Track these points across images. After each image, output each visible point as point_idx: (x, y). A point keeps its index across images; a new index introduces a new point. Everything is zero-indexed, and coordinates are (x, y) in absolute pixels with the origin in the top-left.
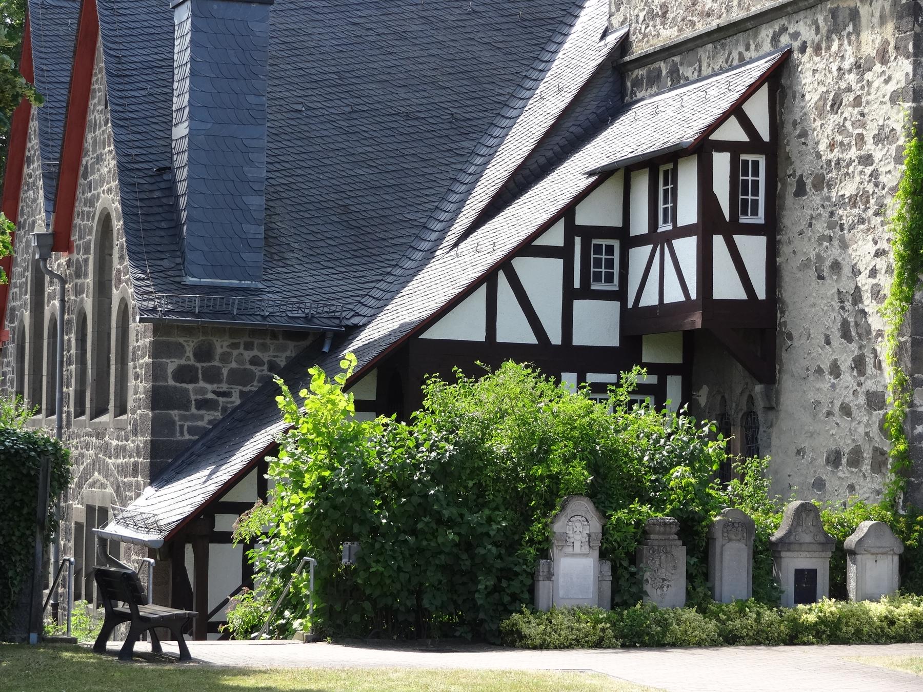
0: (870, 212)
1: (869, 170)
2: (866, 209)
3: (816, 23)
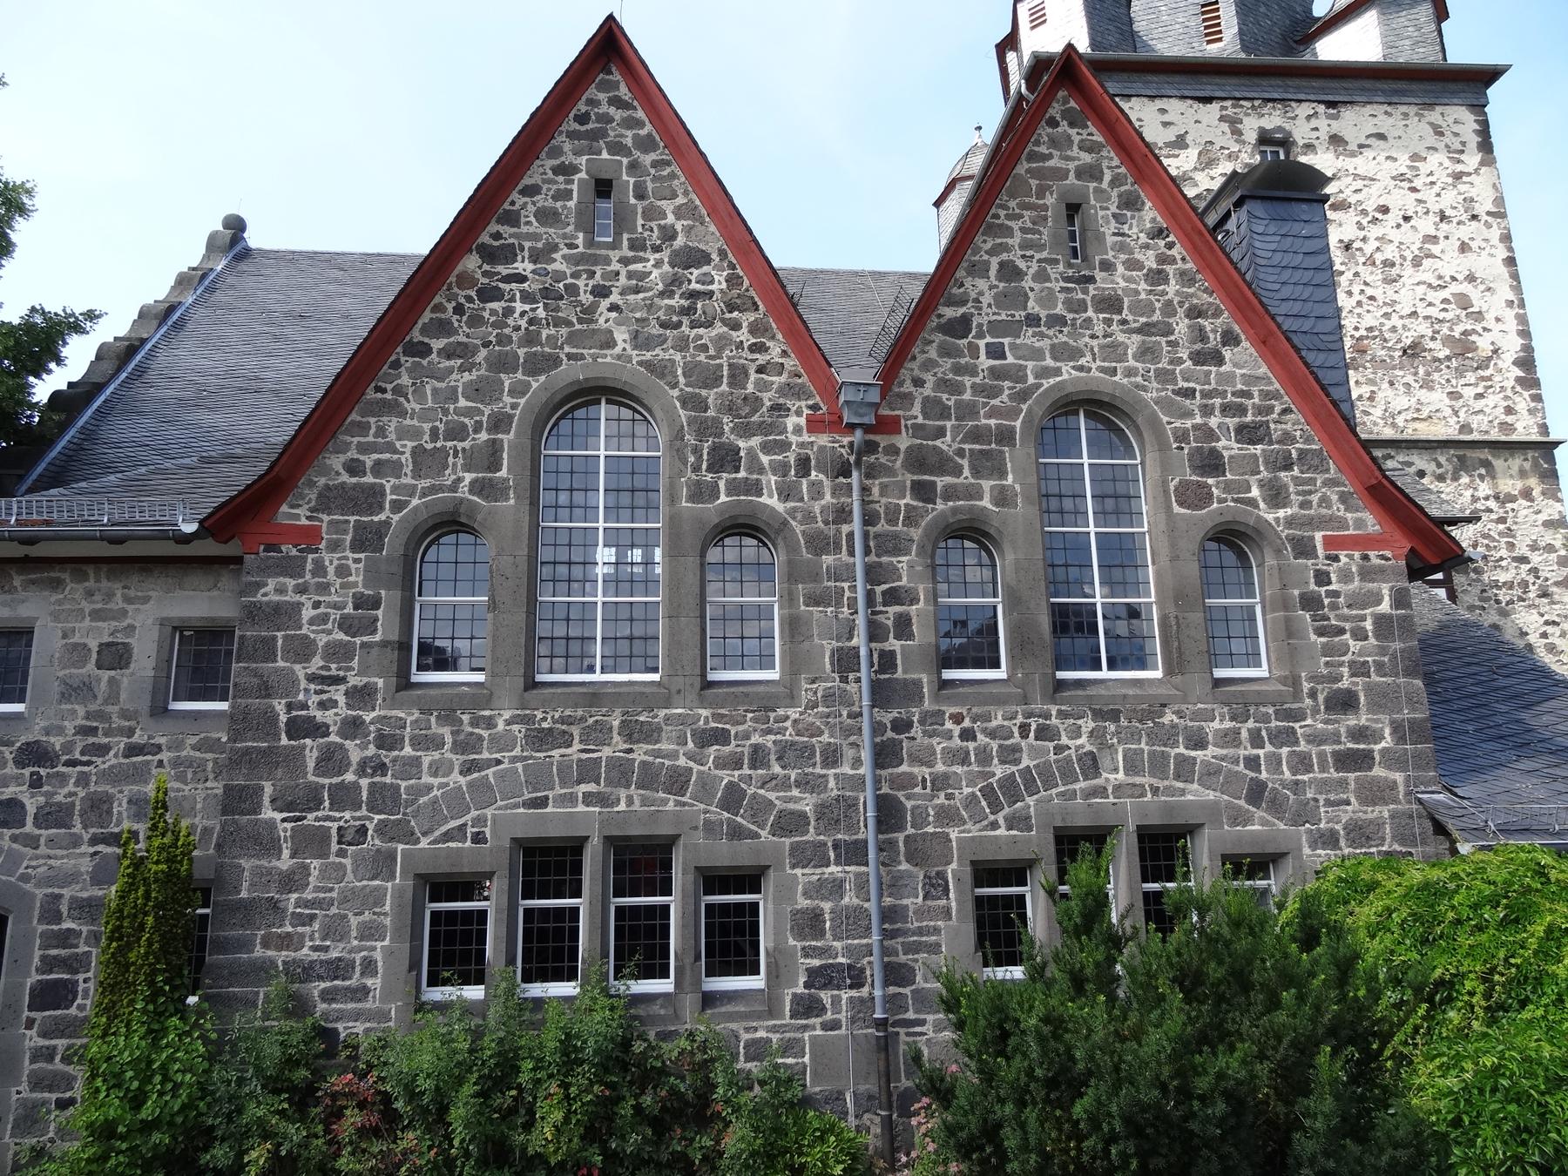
2: (1525, 592)
3: (1435, 460)
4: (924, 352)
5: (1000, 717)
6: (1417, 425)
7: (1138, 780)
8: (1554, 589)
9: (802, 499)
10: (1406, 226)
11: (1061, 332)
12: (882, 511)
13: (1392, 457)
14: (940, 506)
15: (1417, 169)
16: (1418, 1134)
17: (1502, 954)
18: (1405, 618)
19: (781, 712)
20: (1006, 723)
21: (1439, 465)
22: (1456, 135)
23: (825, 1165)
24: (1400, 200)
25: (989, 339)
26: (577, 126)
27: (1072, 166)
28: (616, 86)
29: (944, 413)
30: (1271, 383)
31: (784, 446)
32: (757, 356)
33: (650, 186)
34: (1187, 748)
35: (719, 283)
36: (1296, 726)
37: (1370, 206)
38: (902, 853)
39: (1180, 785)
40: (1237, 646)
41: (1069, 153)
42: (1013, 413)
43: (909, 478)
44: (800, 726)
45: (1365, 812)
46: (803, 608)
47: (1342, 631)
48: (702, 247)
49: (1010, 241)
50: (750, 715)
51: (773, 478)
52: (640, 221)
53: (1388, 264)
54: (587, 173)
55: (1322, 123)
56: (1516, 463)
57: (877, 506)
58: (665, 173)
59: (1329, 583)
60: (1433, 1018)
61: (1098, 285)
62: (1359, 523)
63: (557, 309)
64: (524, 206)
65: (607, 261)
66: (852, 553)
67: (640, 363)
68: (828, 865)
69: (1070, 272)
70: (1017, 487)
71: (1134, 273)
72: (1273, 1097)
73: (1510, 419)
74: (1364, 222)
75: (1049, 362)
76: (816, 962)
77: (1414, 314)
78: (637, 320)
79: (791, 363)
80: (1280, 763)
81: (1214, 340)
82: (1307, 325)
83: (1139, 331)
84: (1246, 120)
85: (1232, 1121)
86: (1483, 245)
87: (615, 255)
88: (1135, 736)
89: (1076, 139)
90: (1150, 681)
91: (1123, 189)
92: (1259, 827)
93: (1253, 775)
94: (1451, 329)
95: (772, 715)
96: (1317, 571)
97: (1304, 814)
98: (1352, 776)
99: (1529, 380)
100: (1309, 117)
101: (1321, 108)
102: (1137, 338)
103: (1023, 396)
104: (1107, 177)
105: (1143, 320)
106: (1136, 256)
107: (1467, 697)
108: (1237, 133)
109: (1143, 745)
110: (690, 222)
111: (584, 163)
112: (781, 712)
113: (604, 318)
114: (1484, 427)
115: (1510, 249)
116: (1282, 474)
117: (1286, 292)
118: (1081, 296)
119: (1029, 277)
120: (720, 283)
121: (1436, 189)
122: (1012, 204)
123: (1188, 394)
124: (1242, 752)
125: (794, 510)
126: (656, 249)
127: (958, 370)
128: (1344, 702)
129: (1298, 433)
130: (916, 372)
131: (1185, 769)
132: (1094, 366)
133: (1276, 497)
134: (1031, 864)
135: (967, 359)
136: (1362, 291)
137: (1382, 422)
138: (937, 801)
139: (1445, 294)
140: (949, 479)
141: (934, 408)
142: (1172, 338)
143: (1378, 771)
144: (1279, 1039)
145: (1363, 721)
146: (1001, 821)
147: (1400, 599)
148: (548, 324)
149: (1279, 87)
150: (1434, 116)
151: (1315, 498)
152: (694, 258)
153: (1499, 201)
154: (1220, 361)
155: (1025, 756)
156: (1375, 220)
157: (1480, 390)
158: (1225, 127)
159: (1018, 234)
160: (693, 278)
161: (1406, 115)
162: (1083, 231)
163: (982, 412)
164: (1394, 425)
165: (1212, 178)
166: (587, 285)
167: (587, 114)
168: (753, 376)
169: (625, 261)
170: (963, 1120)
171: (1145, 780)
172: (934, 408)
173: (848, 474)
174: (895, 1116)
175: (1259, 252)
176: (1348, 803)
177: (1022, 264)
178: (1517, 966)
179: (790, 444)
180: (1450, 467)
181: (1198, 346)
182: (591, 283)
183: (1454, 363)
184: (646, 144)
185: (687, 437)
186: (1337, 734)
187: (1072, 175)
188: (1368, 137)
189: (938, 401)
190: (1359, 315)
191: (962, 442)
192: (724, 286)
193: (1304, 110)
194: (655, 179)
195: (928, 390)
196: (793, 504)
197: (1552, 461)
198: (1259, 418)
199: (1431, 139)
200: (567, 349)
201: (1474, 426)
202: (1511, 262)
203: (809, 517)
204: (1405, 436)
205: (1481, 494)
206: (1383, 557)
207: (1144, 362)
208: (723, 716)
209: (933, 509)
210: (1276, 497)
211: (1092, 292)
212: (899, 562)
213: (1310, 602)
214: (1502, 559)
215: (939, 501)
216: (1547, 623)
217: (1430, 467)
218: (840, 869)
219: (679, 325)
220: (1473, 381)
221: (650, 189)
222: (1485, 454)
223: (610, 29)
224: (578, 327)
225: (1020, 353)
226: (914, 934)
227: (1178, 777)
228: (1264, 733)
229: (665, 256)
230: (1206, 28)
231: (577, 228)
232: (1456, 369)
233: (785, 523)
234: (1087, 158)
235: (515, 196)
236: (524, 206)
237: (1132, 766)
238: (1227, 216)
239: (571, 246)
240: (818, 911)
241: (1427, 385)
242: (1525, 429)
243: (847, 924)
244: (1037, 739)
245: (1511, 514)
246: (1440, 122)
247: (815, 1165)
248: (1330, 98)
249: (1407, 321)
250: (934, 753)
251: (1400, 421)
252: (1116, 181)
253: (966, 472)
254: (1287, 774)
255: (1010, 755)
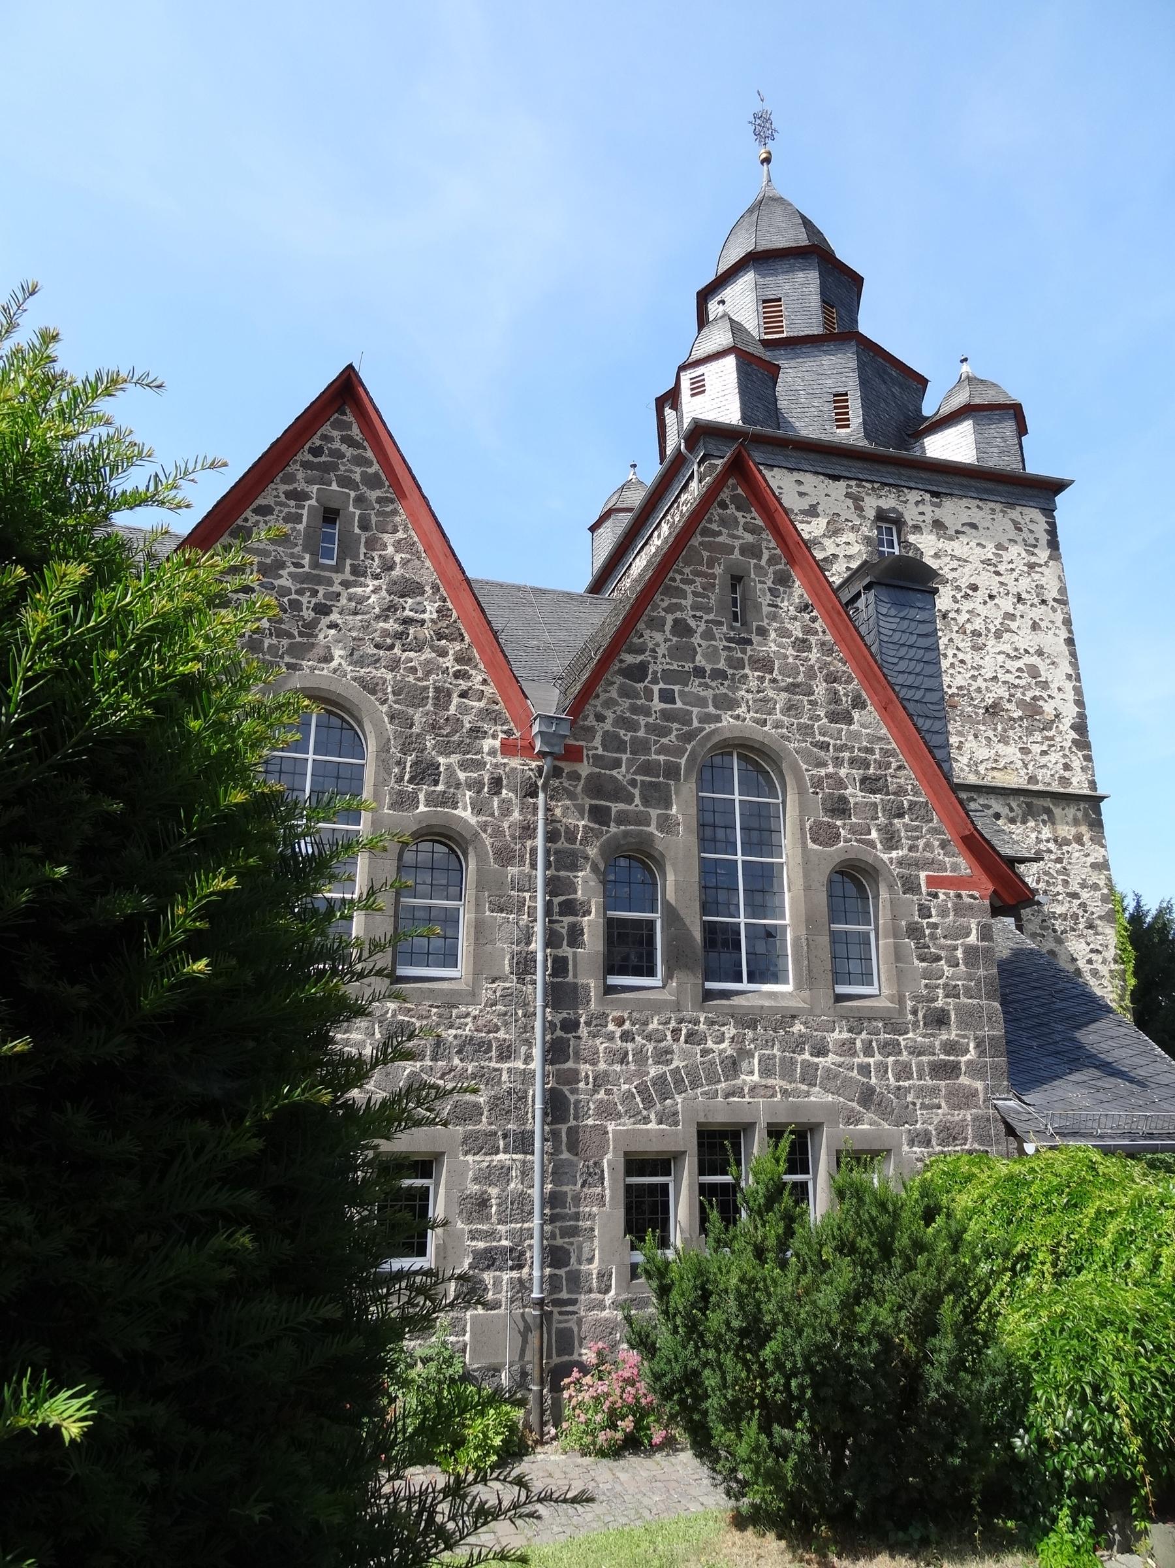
0: (1081, 926)
1: (1076, 902)
2: (1076, 924)
3: (1009, 805)
4: (606, 691)
5: (655, 1021)
6: (995, 774)
7: (770, 1082)
8: (1098, 922)
9: (492, 815)
10: (991, 604)
11: (722, 684)
12: (562, 830)
13: (975, 800)
14: (613, 829)
15: (1001, 556)
16: (1009, 1365)
17: (1065, 1233)
18: (987, 950)
19: (463, 1009)
20: (660, 1027)
21: (1012, 810)
22: (1031, 531)
23: (486, 1436)
24: (986, 581)
25: (662, 685)
26: (311, 458)
27: (737, 543)
28: (349, 426)
29: (621, 747)
30: (889, 743)
31: (480, 765)
32: (461, 682)
33: (374, 519)
34: (812, 1055)
35: (430, 612)
36: (901, 1038)
37: (963, 583)
38: (564, 1144)
39: (805, 1087)
40: (854, 966)
41: (735, 532)
42: (679, 752)
43: (588, 802)
44: (479, 1022)
45: (953, 1115)
46: (488, 913)
47: (938, 958)
48: (416, 578)
49: (683, 602)
50: (434, 1010)
51: (468, 794)
52: (363, 550)
53: (976, 634)
54: (317, 501)
55: (927, 509)
56: (1071, 812)
57: (559, 825)
58: (388, 509)
59: (930, 916)
60: (1014, 1283)
61: (754, 646)
62: (955, 866)
63: (281, 621)
64: (256, 524)
65: (330, 583)
66: (534, 866)
67: (355, 679)
68: (497, 1153)
69: (732, 634)
70: (680, 818)
71: (784, 640)
72: (907, 1341)
73: (1067, 774)
74: (959, 596)
75: (711, 709)
76: (481, 1245)
77: (995, 678)
78: (354, 639)
79: (489, 690)
80: (886, 1072)
81: (846, 702)
82: (918, 695)
83: (786, 689)
84: (867, 498)
85: (882, 1357)
86: (1050, 625)
87: (337, 578)
88: (768, 1043)
89: (742, 521)
90: (783, 995)
91: (778, 567)
92: (867, 1126)
93: (865, 1080)
94: (1024, 695)
95: (455, 1012)
96: (920, 905)
97: (904, 1117)
98: (943, 1083)
99: (1082, 744)
100: (917, 503)
101: (927, 497)
102: (784, 695)
103: (688, 737)
104: (765, 557)
105: (791, 680)
106: (788, 626)
107: (1033, 1017)
108: (859, 509)
109: (775, 1051)
110: (408, 556)
111: (315, 491)
112: (463, 1009)
113: (326, 635)
114: (1047, 781)
115: (1070, 631)
116: (896, 821)
117: (903, 666)
118: (740, 655)
119: (697, 635)
120: (431, 613)
121: (1015, 574)
122: (687, 570)
123: (824, 746)
124: (856, 1060)
125: (486, 824)
126: (376, 577)
127: (635, 709)
128: (939, 1020)
129: (909, 787)
130: (599, 709)
131: (809, 1075)
132: (748, 716)
133: (891, 841)
134: (678, 1156)
135: (643, 701)
136: (955, 655)
137: (967, 769)
138: (597, 1097)
139: (1019, 664)
140: (622, 806)
141: (613, 742)
142: (812, 698)
143: (964, 1080)
144: (914, 1292)
145: (953, 1037)
146: (653, 1116)
147: (985, 933)
148: (271, 634)
149: (894, 474)
150: (1015, 514)
151: (921, 843)
152: (409, 589)
153: (1063, 590)
154: (850, 721)
155: (676, 1057)
156: (966, 596)
157: (1045, 748)
158: (850, 502)
159: (690, 596)
160: (407, 606)
161: (993, 510)
162: (744, 599)
163: (653, 749)
164: (977, 772)
165: (838, 545)
166: (309, 602)
167: (321, 448)
168: (455, 700)
169: (346, 584)
170: (667, 1368)
171: (776, 1082)
172: (613, 742)
173: (534, 795)
174: (545, 1391)
175: (882, 630)
176: (939, 1107)
177: (692, 623)
178: (1075, 1241)
179: (485, 764)
180: (1020, 812)
181: (832, 707)
182: (314, 600)
183: (1025, 724)
184: (373, 482)
185: (393, 750)
186: (932, 1046)
187: (737, 551)
188: (963, 525)
189: (616, 736)
190: (952, 675)
191: (635, 773)
192: (435, 616)
193: (913, 496)
194: (379, 514)
195: (608, 726)
196: (484, 818)
197: (1098, 812)
198: (879, 772)
199: (1012, 534)
200: (287, 659)
201: (1040, 778)
202: (1070, 642)
203: (498, 833)
204: (985, 783)
205: (1043, 837)
206: (972, 896)
207: (789, 716)
208: (410, 1010)
209: (607, 832)
210: (891, 841)
211: (749, 653)
212: (576, 877)
213: (914, 931)
214: (1058, 894)
215: (612, 824)
216: (1092, 951)
217: (1004, 811)
218: (507, 1156)
219: (391, 647)
220: (1039, 739)
221: (373, 522)
222: (1047, 803)
223: (349, 378)
224: (298, 639)
225: (687, 700)
226: (570, 1219)
227: (803, 1081)
228: (874, 1044)
229: (383, 583)
230: (837, 414)
231: (305, 550)
232: (1027, 728)
233: (476, 834)
234: (750, 538)
235: (248, 513)
236: (256, 524)
237: (766, 1071)
238: (858, 595)
239: (298, 565)
240: (486, 1196)
241: (1004, 740)
242: (1078, 784)
243: (512, 1210)
244: (686, 1042)
245: (1066, 856)
246: (1020, 520)
247: (476, 1436)
248: (935, 489)
249: (989, 684)
250: (597, 1053)
251: (981, 769)
252: (772, 561)
253: (637, 801)
254: (892, 1080)
255: (663, 1056)
